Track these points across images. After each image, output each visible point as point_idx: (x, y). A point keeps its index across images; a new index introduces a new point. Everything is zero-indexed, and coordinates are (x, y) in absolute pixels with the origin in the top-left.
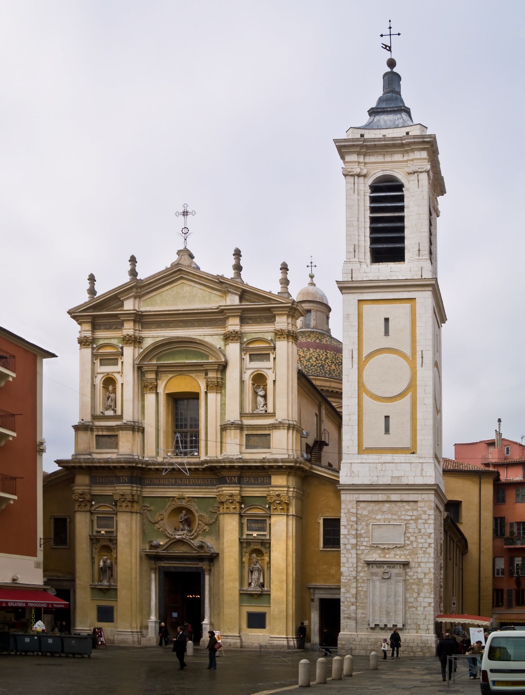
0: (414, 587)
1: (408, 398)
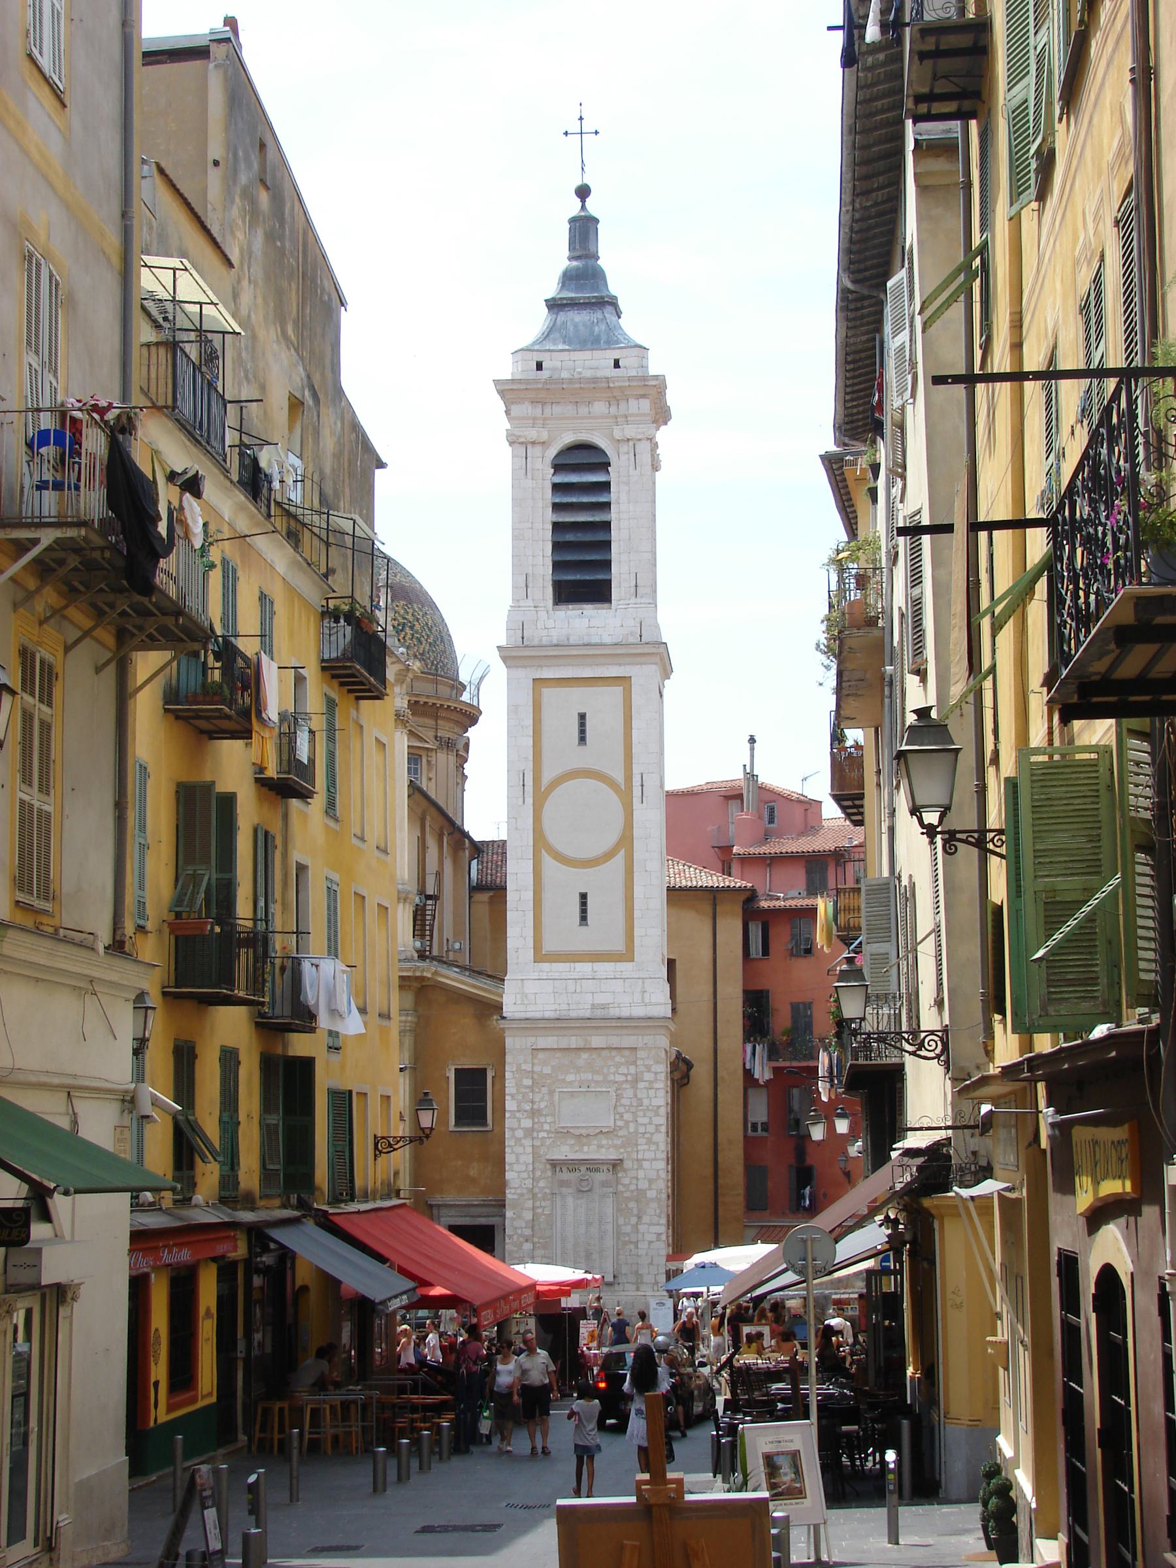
0: (632, 1205)
1: (620, 858)
